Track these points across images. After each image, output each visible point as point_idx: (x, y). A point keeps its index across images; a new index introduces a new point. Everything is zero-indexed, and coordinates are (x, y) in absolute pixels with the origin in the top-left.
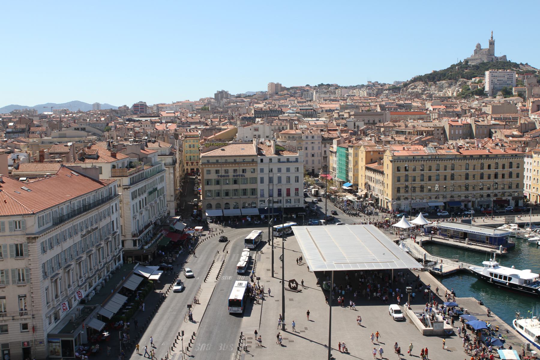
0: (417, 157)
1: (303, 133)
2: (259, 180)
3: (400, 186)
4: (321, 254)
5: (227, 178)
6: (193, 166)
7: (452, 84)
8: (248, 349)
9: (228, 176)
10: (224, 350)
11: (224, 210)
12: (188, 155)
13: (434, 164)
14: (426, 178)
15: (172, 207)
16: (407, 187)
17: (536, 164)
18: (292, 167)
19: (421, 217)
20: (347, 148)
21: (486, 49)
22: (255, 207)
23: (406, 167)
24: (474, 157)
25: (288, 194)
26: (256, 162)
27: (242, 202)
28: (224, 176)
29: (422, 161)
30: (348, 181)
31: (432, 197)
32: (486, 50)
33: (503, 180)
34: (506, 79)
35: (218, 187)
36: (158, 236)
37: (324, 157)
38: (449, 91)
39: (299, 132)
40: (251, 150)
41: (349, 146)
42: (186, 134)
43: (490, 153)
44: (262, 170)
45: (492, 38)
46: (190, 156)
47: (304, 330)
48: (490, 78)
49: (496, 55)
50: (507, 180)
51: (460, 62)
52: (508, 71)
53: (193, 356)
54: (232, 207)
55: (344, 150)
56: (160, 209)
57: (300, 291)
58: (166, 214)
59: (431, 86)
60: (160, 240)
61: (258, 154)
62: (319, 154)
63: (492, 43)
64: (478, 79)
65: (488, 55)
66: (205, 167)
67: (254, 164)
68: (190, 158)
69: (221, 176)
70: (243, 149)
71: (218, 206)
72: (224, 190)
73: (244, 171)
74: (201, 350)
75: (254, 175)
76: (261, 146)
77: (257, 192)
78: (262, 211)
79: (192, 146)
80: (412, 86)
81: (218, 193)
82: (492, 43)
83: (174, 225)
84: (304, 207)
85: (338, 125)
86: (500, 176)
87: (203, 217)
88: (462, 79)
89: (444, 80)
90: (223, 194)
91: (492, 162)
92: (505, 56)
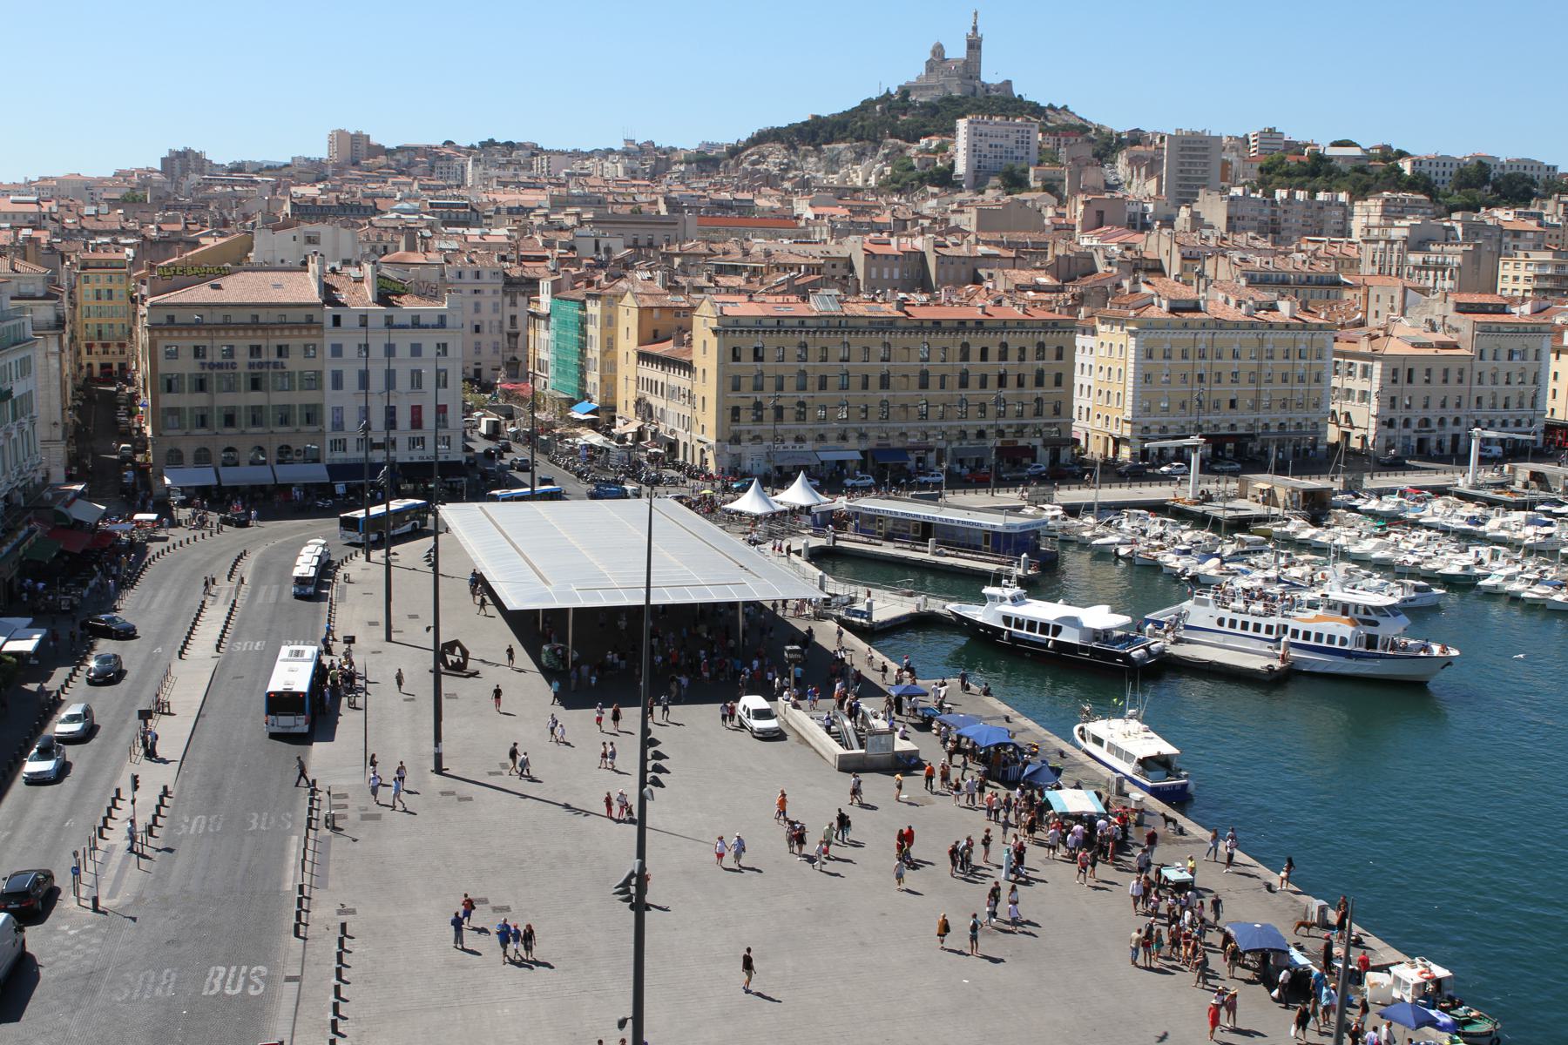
0: (787, 322)
1: (448, 262)
2: (328, 380)
3: (739, 403)
4: (534, 568)
5: (231, 371)
6: (110, 356)
7: (863, 154)
8: (338, 824)
9: (233, 366)
10: (263, 828)
11: (222, 470)
12: (93, 321)
13: (833, 342)
14: (812, 382)
15: (53, 459)
16: (758, 406)
17: (1104, 351)
18: (429, 341)
19: (804, 485)
20: (584, 303)
21: (957, 60)
22: (317, 461)
23: (756, 350)
24: (943, 324)
25: (417, 423)
26: (320, 326)
27: (275, 447)
28: (220, 366)
29: (801, 332)
30: (585, 396)
31: (828, 435)
32: (959, 64)
33: (1020, 391)
34: (1011, 143)
35: (200, 400)
36: (21, 534)
37: (509, 334)
38: (855, 172)
39: (434, 257)
40: (305, 288)
41: (589, 296)
42: (85, 256)
43: (986, 317)
44: (337, 350)
45: (975, 29)
46: (99, 325)
47: (498, 769)
48: (968, 139)
49: (983, 78)
50: (1031, 391)
51: (888, 91)
52: (1017, 121)
53: (170, 850)
54: (246, 454)
55: (572, 310)
56: (20, 459)
57: (475, 674)
58: (39, 476)
59: (805, 156)
60: (26, 544)
61: (325, 302)
62: (496, 324)
63: (974, 45)
64: (935, 142)
65: (961, 76)
66: (161, 337)
67: (314, 332)
68: (100, 332)
69: (212, 366)
70: (277, 286)
71: (202, 457)
72: (219, 409)
73: (281, 351)
74: (192, 832)
75: (309, 366)
76: (332, 280)
77: (322, 415)
78: (336, 471)
79: (104, 294)
80: (752, 154)
81: (203, 417)
82: (974, 45)
83: (67, 507)
84: (464, 461)
85: (549, 244)
86: (1012, 380)
87: (157, 491)
88: (891, 141)
89: (843, 140)
90: (216, 420)
91: (992, 342)
92: (1008, 83)
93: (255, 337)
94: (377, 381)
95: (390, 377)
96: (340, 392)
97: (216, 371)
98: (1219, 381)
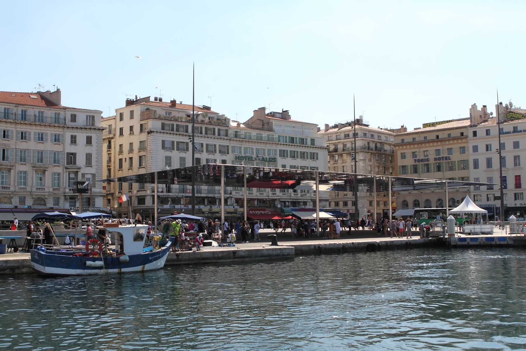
9: (428, 160)
28: (422, 160)
44: (475, 149)
66: (399, 149)
67: (464, 140)
69: (419, 161)
73: (450, 150)
75: (463, 157)
93: (437, 146)
94: (496, 163)
96: (477, 170)
97: (421, 163)
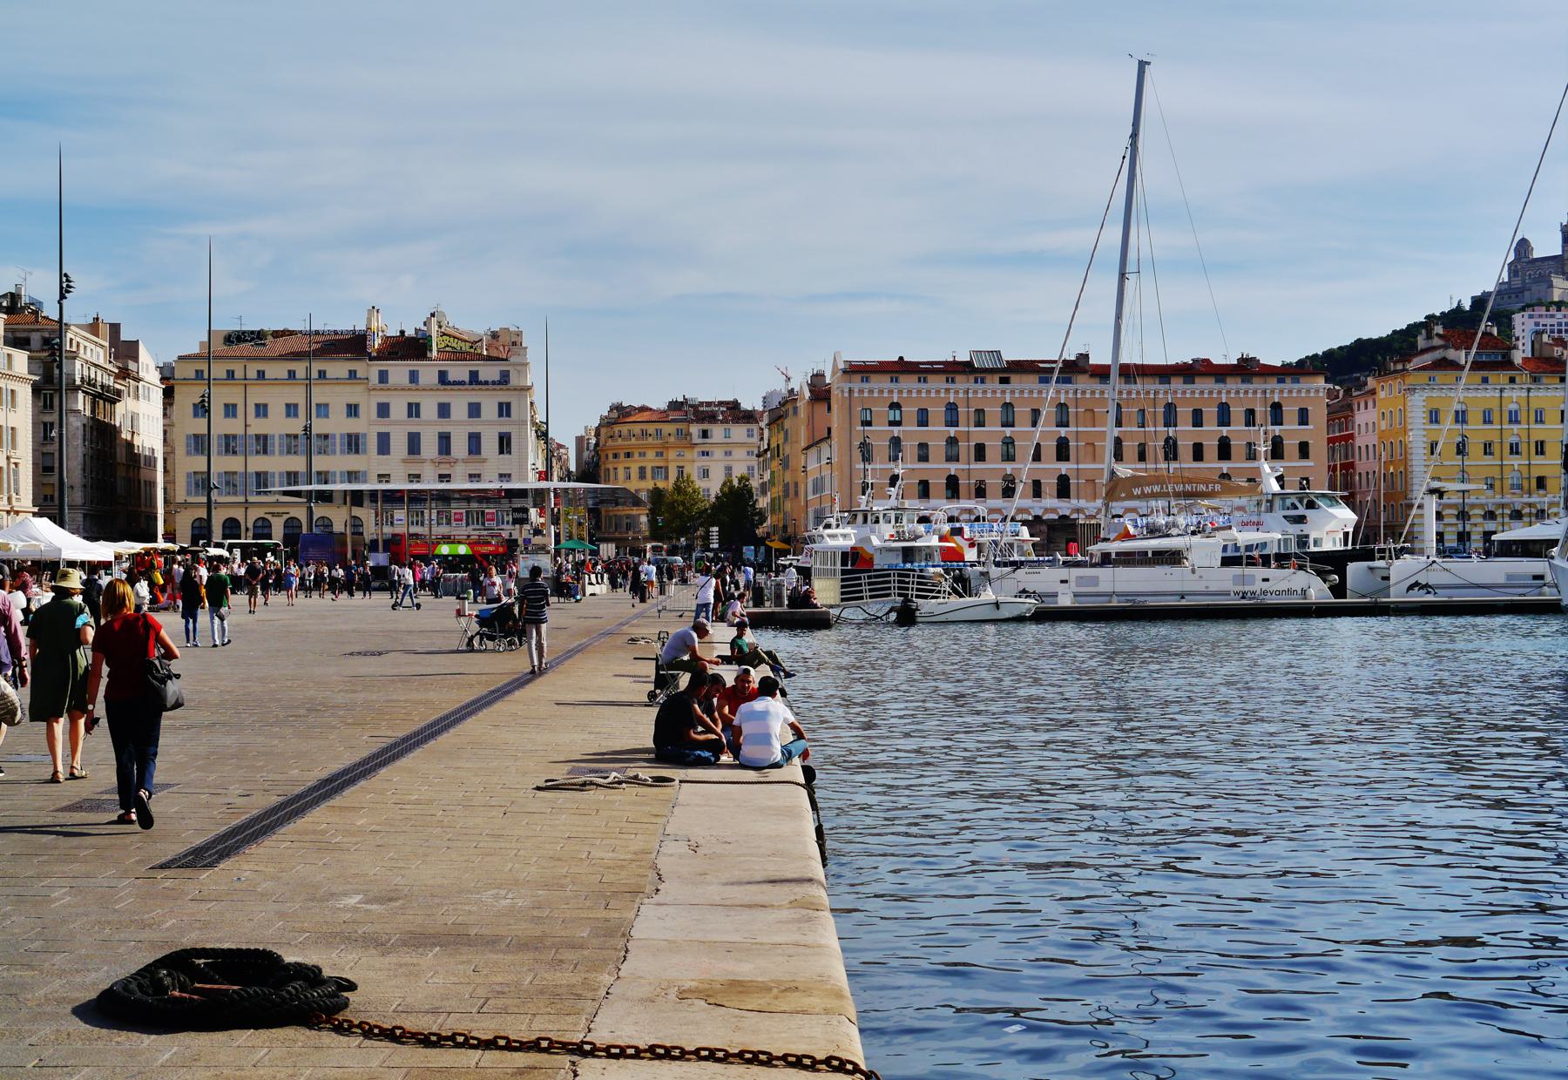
95: (445, 441)
98: (1542, 453)
